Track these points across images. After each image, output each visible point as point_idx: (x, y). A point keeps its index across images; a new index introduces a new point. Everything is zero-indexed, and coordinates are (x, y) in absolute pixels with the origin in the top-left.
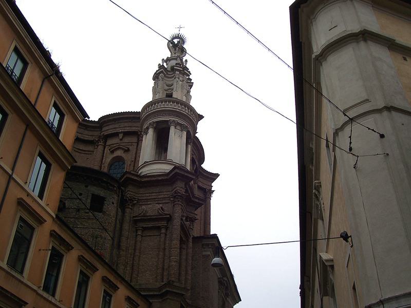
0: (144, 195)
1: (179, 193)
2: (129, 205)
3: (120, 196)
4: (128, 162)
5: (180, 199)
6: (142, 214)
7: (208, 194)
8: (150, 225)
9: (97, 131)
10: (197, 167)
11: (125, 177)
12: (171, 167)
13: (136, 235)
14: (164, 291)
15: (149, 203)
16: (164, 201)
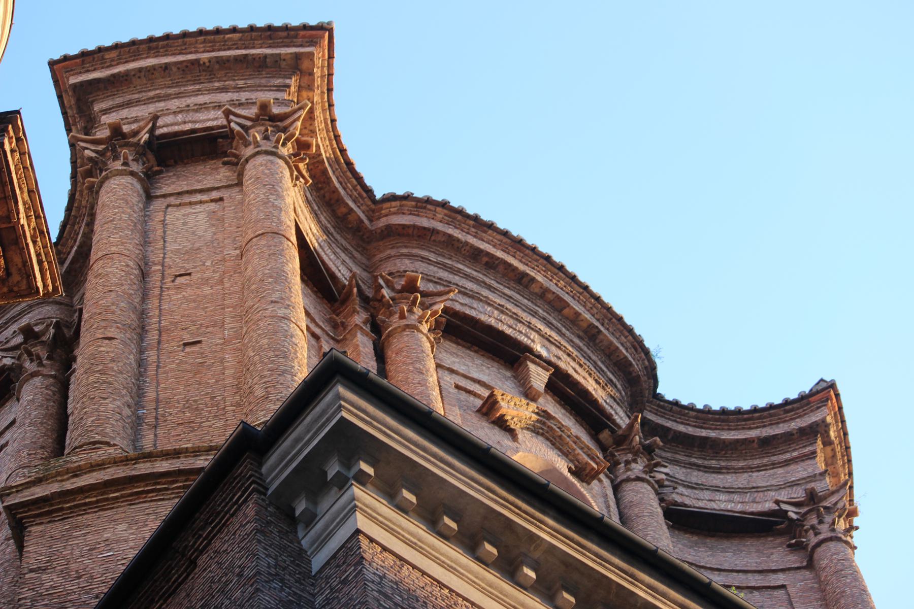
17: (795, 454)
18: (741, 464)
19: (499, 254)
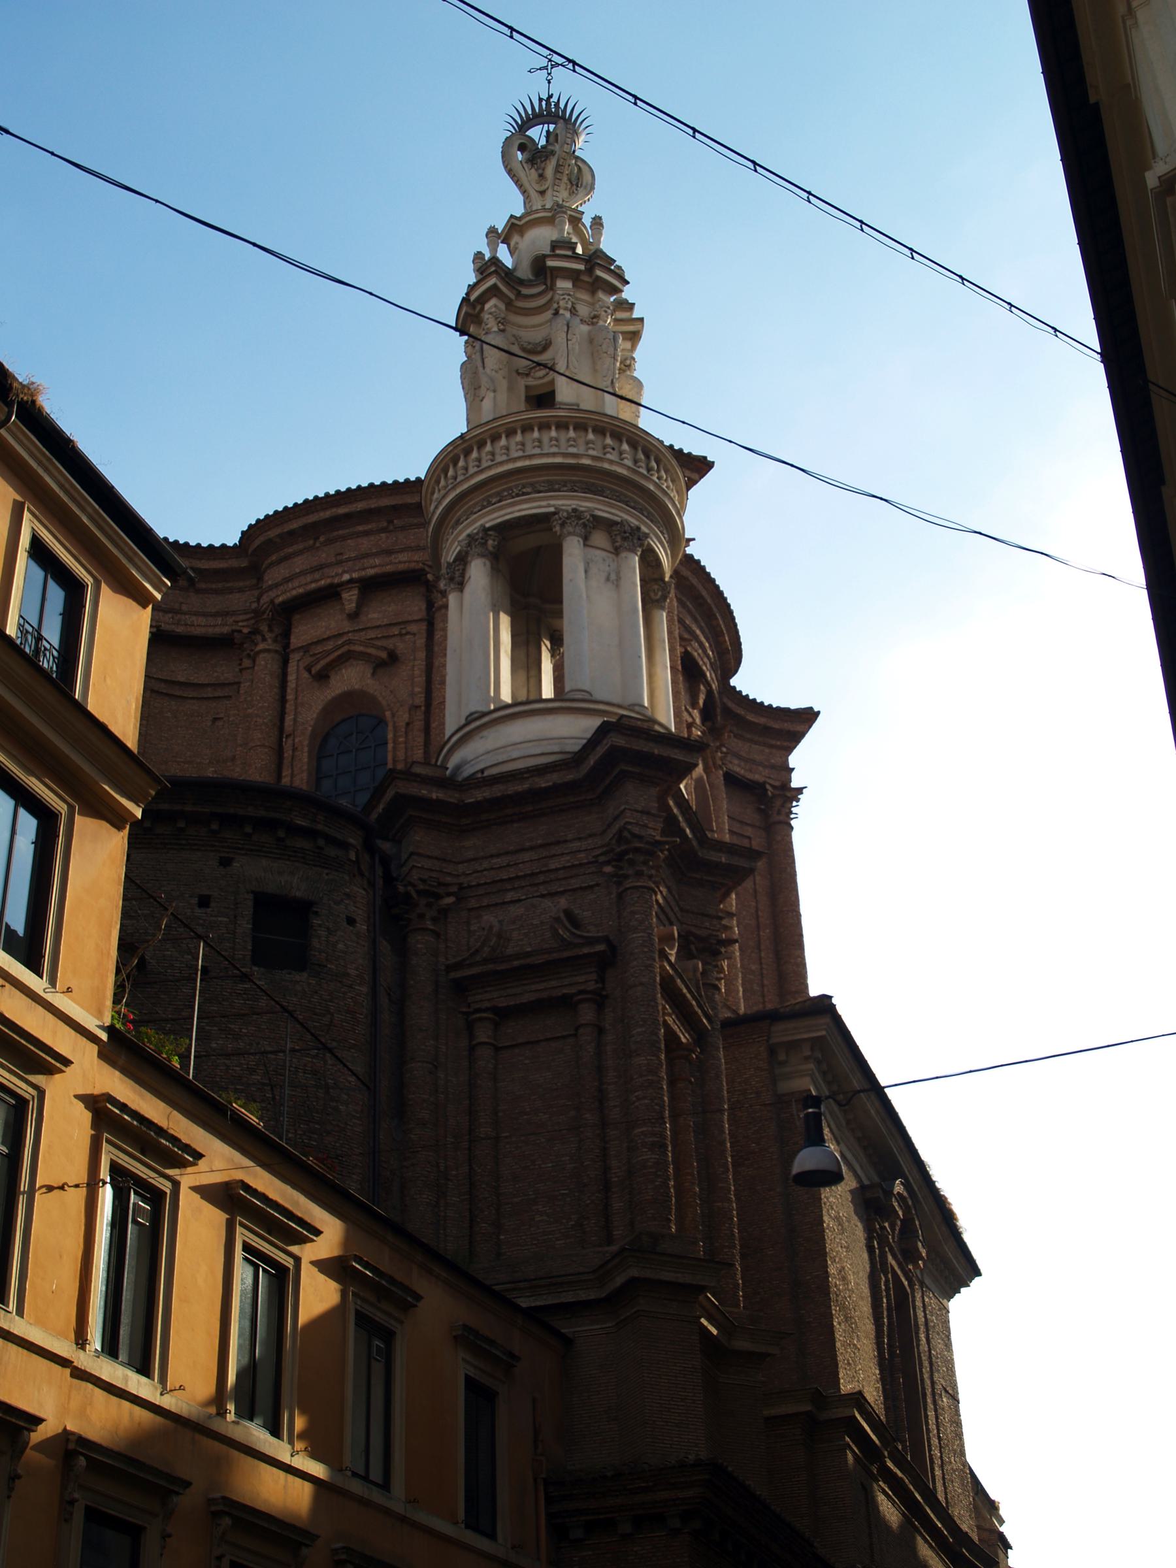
0: (485, 865)
1: (640, 838)
2: (421, 916)
3: (380, 882)
5: (645, 863)
6: (486, 949)
7: (778, 803)
8: (528, 992)
9: (240, 590)
10: (710, 693)
11: (390, 794)
12: (593, 723)
13: (472, 1049)
14: (619, 1281)
15: (509, 896)
16: (575, 883)
17: (779, 743)
18: (749, 736)
19: (709, 601)
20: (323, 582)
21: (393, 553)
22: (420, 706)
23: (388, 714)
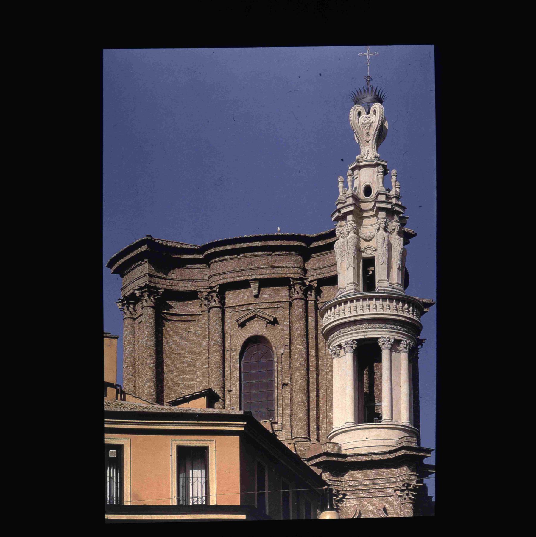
4: (278, 350)
20: (242, 278)
21: (275, 268)
22: (287, 345)
23: (274, 348)
